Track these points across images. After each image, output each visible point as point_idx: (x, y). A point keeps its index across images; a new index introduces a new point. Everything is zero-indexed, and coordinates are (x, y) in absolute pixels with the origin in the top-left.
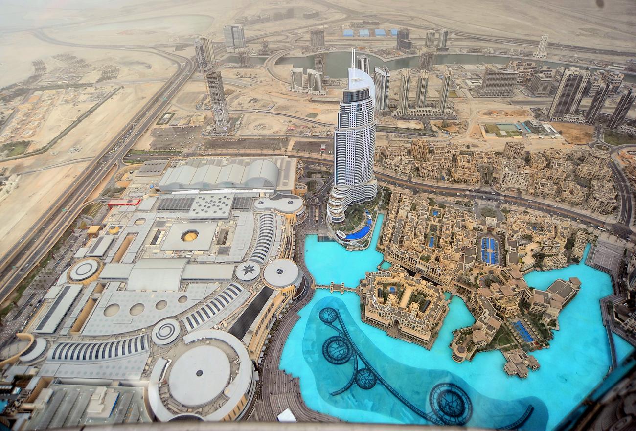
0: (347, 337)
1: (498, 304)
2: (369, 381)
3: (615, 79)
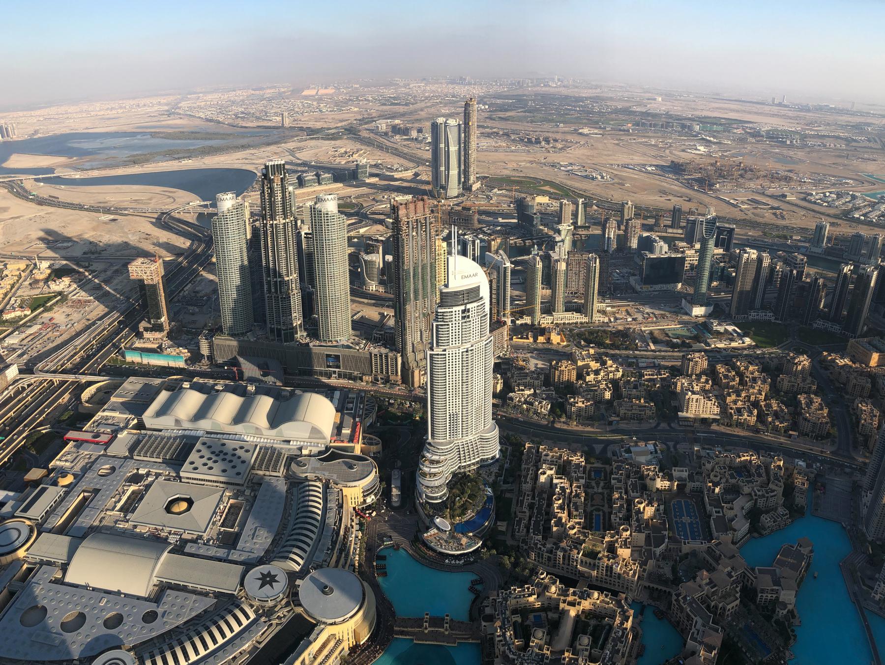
1: (713, 604)
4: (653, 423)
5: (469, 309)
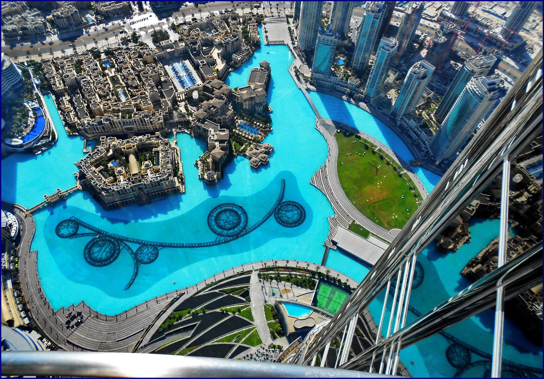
0: (102, 234)
2: (151, 254)
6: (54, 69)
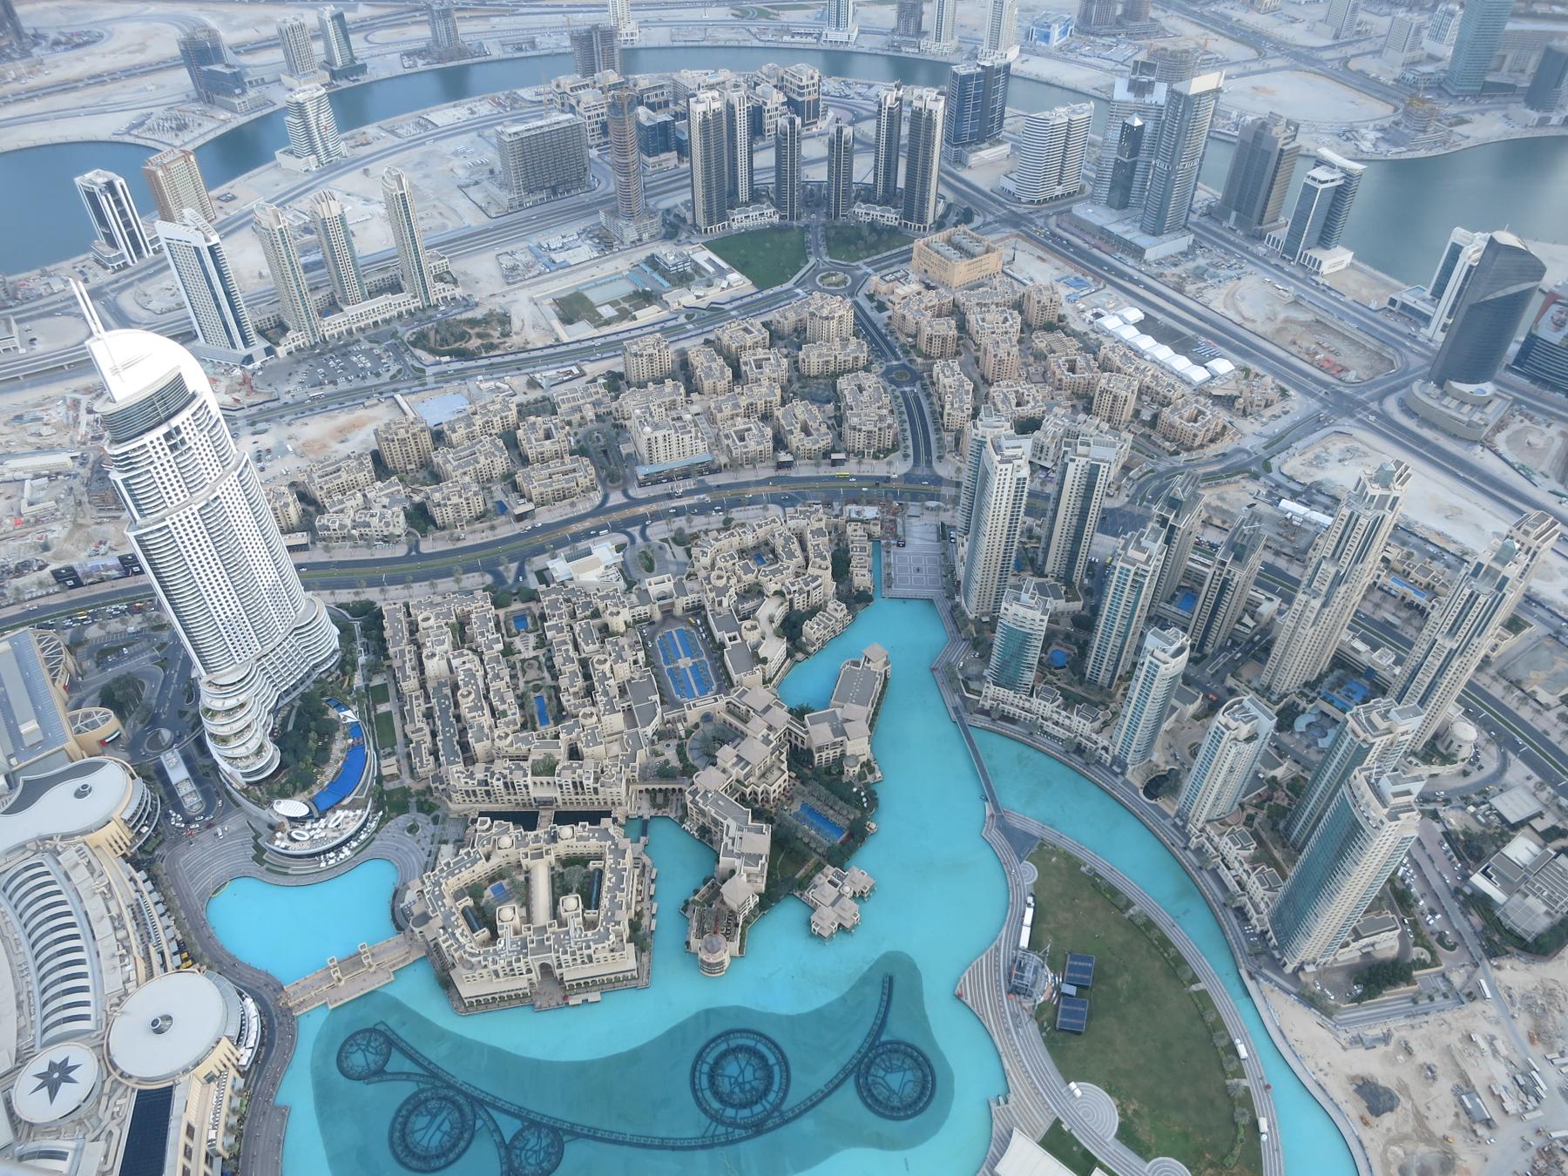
0: (440, 1079)
1: (748, 791)
3: (804, 83)
4: (596, 498)
5: (178, 430)
6: (405, 626)
